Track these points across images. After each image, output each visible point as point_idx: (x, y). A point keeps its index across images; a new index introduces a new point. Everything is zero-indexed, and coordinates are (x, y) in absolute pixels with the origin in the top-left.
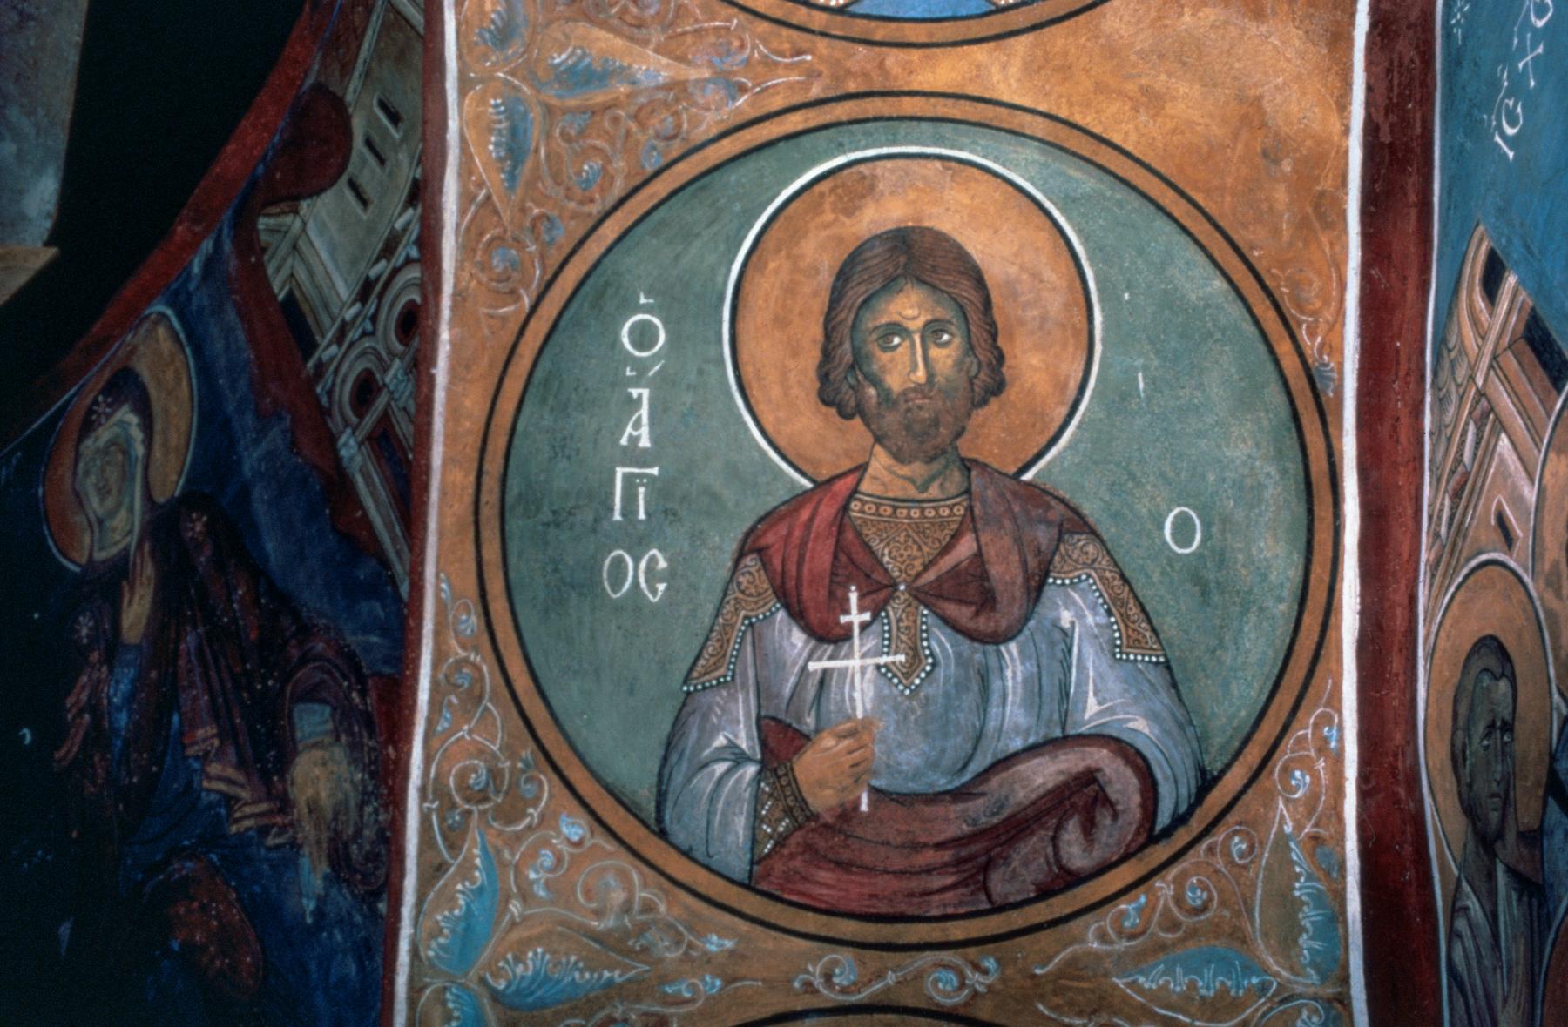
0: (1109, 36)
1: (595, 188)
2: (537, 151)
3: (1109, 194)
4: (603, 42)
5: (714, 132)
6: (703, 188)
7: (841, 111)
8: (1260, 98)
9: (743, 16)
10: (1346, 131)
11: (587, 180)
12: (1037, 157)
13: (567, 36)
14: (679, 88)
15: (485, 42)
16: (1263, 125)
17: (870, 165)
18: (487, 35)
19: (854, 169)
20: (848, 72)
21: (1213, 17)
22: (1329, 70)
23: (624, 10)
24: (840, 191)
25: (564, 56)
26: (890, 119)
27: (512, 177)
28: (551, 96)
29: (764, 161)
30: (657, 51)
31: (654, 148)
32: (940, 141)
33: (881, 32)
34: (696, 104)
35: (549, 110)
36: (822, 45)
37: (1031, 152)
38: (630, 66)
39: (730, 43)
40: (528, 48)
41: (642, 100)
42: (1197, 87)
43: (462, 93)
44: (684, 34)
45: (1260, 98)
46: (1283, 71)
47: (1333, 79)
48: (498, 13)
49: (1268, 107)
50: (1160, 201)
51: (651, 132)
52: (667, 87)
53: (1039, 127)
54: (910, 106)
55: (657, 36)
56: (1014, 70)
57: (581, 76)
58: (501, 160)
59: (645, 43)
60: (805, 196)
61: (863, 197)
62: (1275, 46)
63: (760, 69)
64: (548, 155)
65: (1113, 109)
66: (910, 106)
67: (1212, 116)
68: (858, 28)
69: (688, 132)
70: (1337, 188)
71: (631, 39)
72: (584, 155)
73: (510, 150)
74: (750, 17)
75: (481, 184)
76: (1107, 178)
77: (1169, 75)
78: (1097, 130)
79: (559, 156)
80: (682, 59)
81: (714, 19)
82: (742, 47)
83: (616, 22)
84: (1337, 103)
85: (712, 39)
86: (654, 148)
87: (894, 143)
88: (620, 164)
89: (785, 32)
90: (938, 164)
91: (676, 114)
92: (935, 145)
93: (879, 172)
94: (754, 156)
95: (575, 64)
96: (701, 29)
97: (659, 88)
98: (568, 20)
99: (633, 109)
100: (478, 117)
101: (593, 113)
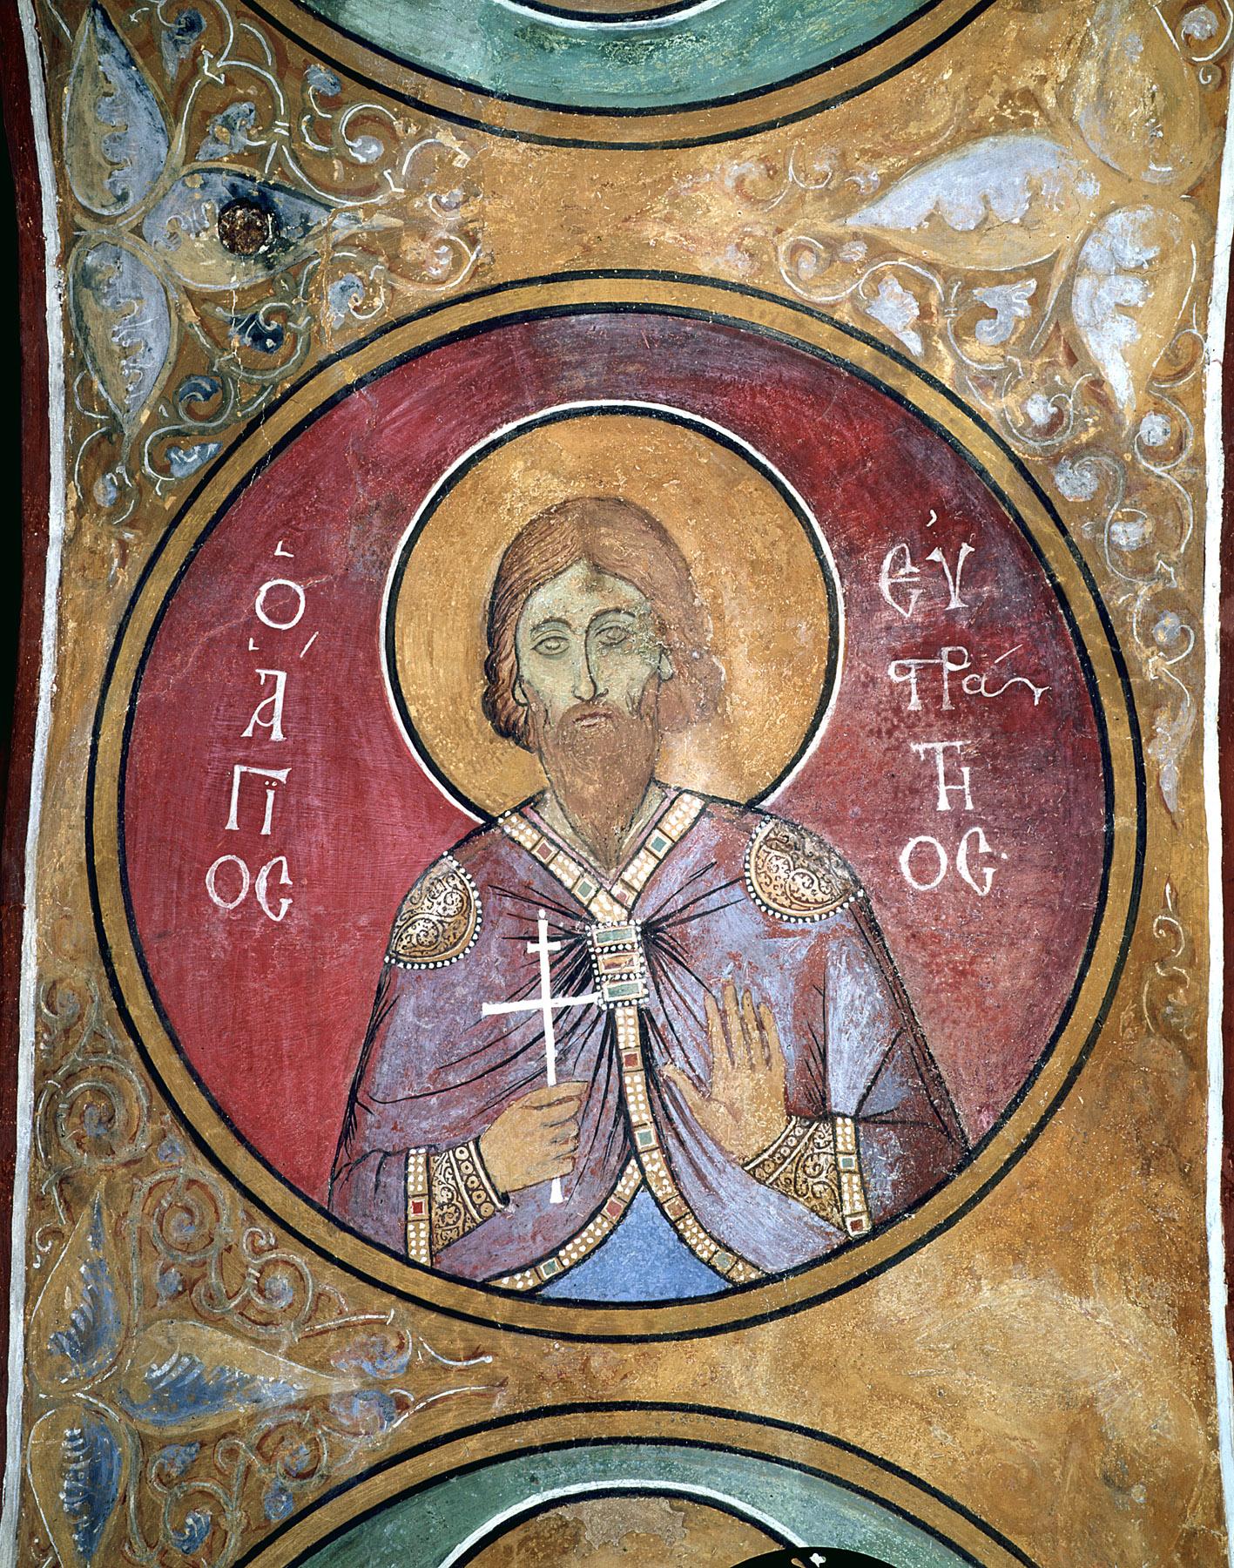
0: (885, 1320)
1: (201, 1549)
2: (124, 1499)
3: (898, 1540)
4: (217, 1348)
5: (364, 1465)
6: (350, 1543)
7: (534, 1432)
8: (1091, 1401)
9: (403, 1306)
10: (1215, 1443)
11: (191, 1539)
12: (797, 1491)
13: (171, 1342)
14: (316, 1405)
15: (63, 1352)
16: (1102, 1437)
17: (572, 1506)
18: (65, 1342)
19: (551, 1513)
20: (542, 1377)
21: (1020, 1292)
22: (1181, 1359)
23: (247, 1301)
24: (532, 1544)
25: (166, 1368)
26: (598, 1442)
27: (89, 1537)
28: (147, 1423)
29: (431, 1505)
30: (288, 1356)
31: (283, 1490)
32: (666, 1471)
33: (584, 1322)
34: (341, 1429)
35: (144, 1443)
36: (506, 1340)
37: (790, 1484)
38: (253, 1378)
39: (386, 1342)
40: (118, 1357)
41: (268, 1423)
42: (1006, 1386)
43: (27, 1421)
44: (325, 1331)
45: (1091, 1401)
46: (1120, 1361)
47: (1191, 1372)
48: (82, 1312)
49: (1102, 1410)
50: (969, 1549)
51: (279, 1467)
52: (301, 1406)
53: (798, 1449)
54: (625, 1423)
55: (288, 1335)
56: (762, 1368)
57: (189, 1394)
58: (75, 1514)
59: (273, 1346)
60: (486, 1553)
61: (565, 1551)
62: (1105, 1327)
63: (426, 1377)
64: (139, 1507)
65: (897, 1420)
66: (625, 1423)
67: (1029, 1426)
68: (554, 1318)
69: (328, 1467)
70: (1211, 1526)
71: (256, 1341)
72: (189, 1502)
73: (89, 1500)
74: (412, 1307)
75: (44, 1550)
76: (893, 1517)
77: (968, 1370)
78: (877, 1451)
79: (155, 1507)
80: (322, 1366)
81: (365, 1312)
82: (401, 1347)
83: (235, 1319)
84: (1198, 1404)
85: (361, 1338)
86: (283, 1490)
87: (604, 1475)
88: (235, 1517)
89: (458, 1325)
90: (664, 1503)
91: (314, 1442)
92: (660, 1476)
93: (585, 1517)
94: (417, 1498)
95: (181, 1378)
96: (348, 1325)
97: (291, 1407)
98: (173, 1318)
99: (255, 1437)
100: (47, 1454)
101: (203, 1445)
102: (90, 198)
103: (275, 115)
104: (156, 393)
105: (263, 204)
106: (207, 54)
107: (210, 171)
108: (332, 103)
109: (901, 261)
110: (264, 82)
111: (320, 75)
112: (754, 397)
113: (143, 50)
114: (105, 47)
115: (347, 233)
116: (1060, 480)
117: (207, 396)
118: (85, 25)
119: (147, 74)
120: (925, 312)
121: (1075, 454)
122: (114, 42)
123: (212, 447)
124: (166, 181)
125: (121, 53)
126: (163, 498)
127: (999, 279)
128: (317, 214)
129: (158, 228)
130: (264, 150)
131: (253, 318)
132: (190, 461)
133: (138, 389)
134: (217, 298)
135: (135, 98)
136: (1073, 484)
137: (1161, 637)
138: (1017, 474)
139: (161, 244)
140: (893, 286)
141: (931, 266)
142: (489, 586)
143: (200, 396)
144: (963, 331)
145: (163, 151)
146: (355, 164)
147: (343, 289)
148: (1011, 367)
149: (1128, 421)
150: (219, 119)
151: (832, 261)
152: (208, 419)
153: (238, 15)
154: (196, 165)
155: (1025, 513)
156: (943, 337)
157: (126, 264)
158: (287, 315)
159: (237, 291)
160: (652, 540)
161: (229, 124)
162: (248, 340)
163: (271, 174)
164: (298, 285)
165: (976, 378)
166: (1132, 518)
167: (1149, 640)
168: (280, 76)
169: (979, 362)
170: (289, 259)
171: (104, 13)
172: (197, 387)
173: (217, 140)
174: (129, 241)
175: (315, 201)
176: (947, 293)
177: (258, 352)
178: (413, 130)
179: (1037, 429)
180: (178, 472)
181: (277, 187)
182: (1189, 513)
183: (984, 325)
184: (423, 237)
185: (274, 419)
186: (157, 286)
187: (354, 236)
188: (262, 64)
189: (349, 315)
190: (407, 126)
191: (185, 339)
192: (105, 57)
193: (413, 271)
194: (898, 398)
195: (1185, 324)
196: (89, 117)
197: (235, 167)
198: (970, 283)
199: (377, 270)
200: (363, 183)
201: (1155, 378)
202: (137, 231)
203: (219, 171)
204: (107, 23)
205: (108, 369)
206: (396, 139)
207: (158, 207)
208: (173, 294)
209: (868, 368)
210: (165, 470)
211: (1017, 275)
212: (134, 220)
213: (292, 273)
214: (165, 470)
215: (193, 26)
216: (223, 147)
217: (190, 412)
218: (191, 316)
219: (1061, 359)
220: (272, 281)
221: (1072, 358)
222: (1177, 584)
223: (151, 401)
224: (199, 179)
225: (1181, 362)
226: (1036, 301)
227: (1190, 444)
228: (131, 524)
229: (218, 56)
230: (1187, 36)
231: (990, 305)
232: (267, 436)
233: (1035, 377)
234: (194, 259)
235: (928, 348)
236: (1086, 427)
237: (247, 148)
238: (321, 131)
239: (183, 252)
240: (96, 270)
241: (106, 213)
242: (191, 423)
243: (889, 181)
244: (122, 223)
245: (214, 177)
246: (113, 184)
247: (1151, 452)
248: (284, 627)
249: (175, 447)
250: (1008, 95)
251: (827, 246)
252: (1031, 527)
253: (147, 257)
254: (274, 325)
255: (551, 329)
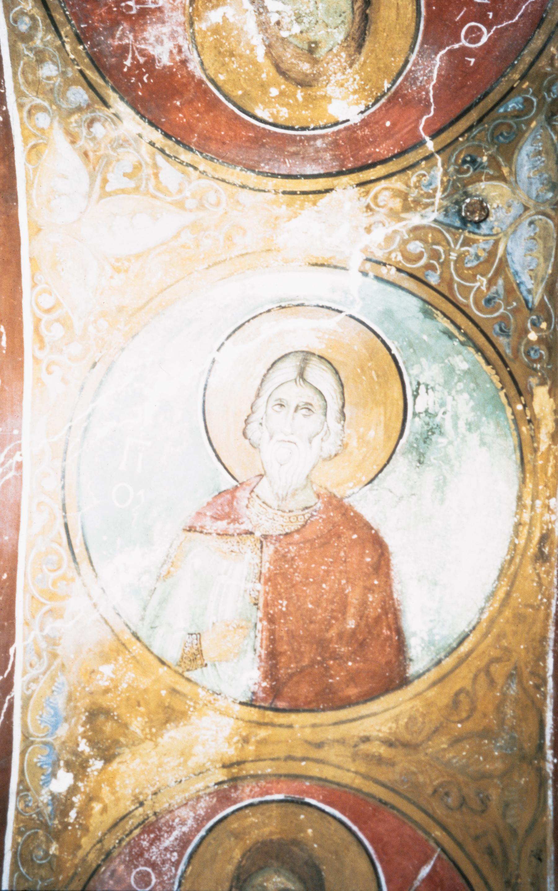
102: (547, 223)
103: (456, 262)
104: (527, 135)
105: (464, 221)
106: (484, 288)
107: (489, 235)
108: (429, 267)
109: (169, 199)
110: (459, 276)
111: (433, 279)
112: (235, 135)
113: (511, 291)
114: (529, 291)
115: (427, 210)
116: (86, 97)
117: (501, 134)
118: (537, 301)
119: (512, 278)
120: (156, 175)
121: (79, 109)
122: (525, 293)
123: (502, 110)
124: (510, 231)
125: (523, 288)
126: (528, 87)
127: (123, 191)
128: (441, 218)
129: (516, 210)
130: (463, 245)
131: (475, 170)
132: (513, 105)
133: (535, 136)
134: (491, 178)
135: (518, 268)
136: (79, 95)
137: (27, 19)
138: (107, 99)
139: (516, 203)
140: (173, 188)
141: (155, 197)
142: (367, 43)
143: (505, 134)
144: (138, 167)
145: (509, 244)
146: (421, 240)
147: (430, 184)
148: (114, 150)
149: (56, 124)
150: (482, 259)
151: (201, 199)
152: (502, 124)
153: (468, 306)
154: (495, 238)
155: (100, 81)
156: (147, 164)
157: (534, 195)
158: (458, 172)
159: (482, 181)
160: (283, 66)
161: (477, 257)
162: (479, 160)
163: (460, 234)
164: (453, 185)
165: (130, 145)
166: (49, 78)
167: (33, 18)
168: (452, 279)
169: (129, 152)
170: (456, 196)
171: (527, 306)
172: (505, 138)
173: (484, 250)
174: (531, 204)
175: (441, 223)
176: (147, 184)
177: (474, 154)
178: (393, 255)
179: (99, 120)
180: (520, 99)
181: (457, 228)
182: (21, 80)
183: (129, 170)
184: (391, 209)
185: (469, 124)
186: (520, 184)
187: (424, 208)
188: (460, 285)
189: (429, 173)
190: (396, 258)
191: (509, 160)
192: (530, 286)
193: (397, 194)
194: (167, 135)
195: (35, 170)
196: (542, 260)
197: (477, 237)
198: (137, 189)
199: (414, 194)
200: (418, 232)
201: (46, 144)
202: (526, 208)
203: (485, 235)
204: (527, 302)
205: (549, 145)
206: (401, 251)
207: (515, 219)
208: (512, 179)
209: (181, 149)
210: (526, 100)
211: (116, 193)
212: (527, 213)
213: (455, 189)
214: (526, 100)
215: (489, 301)
216: (481, 246)
217: (510, 126)
218: (505, 170)
219: (91, 154)
220: (465, 186)
221: (86, 154)
222: (22, 46)
223: (529, 132)
224: (494, 232)
225: (34, 150)
226: (105, 181)
227: (25, 114)
228: (546, 74)
229: (479, 288)
230: (51, 295)
231: (126, 179)
232: (474, 115)
233: (103, 145)
234: (501, 195)
235: (154, 159)
236: (76, 122)
237: (470, 246)
238: (435, 255)
239: (506, 199)
240: (548, 190)
241: (540, 217)
242: (511, 122)
243: (177, 236)
244: (533, 212)
245: (487, 232)
246: (534, 229)
247: (44, 110)
248: (473, 24)
249: (520, 111)
250: (126, 271)
251: (203, 206)
252: (97, 74)
253: (523, 197)
254: (465, 167)
255: (332, 167)
